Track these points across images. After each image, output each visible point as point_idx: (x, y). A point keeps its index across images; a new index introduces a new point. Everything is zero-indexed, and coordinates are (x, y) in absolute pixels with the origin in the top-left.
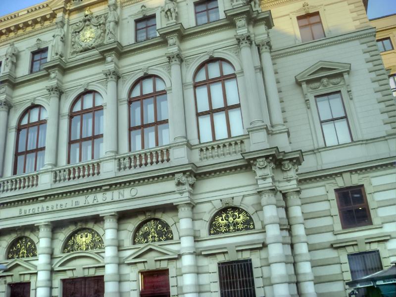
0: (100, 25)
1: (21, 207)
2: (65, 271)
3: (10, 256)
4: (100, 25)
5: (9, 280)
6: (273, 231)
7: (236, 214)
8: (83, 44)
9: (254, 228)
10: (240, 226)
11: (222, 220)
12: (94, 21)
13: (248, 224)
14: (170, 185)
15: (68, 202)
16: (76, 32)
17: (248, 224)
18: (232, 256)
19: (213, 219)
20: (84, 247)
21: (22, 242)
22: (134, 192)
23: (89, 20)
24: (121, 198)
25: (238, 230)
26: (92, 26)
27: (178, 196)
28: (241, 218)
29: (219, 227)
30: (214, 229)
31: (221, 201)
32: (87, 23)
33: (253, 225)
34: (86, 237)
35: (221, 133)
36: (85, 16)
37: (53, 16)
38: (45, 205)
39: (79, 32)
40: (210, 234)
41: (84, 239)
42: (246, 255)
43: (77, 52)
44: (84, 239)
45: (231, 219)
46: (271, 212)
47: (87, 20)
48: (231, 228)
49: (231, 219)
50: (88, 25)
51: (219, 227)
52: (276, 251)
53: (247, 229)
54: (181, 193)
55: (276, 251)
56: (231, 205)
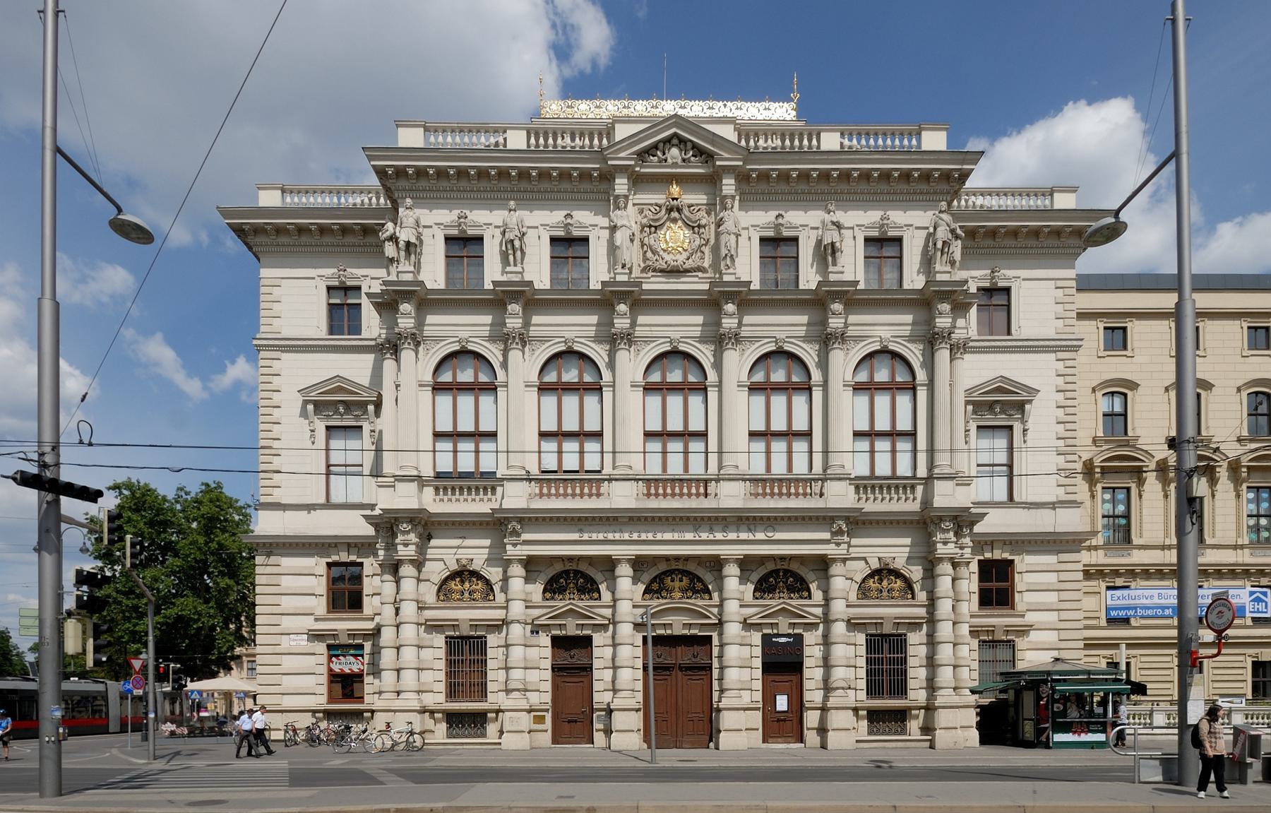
0: (699, 226)
4: (699, 226)
8: (668, 257)
10: (896, 594)
16: (650, 226)
19: (864, 580)
21: (568, 577)
23: (679, 210)
26: (680, 224)
27: (833, 546)
32: (675, 214)
34: (681, 580)
37: (607, 177)
47: (673, 209)
48: (885, 594)
50: (674, 221)
54: (838, 544)
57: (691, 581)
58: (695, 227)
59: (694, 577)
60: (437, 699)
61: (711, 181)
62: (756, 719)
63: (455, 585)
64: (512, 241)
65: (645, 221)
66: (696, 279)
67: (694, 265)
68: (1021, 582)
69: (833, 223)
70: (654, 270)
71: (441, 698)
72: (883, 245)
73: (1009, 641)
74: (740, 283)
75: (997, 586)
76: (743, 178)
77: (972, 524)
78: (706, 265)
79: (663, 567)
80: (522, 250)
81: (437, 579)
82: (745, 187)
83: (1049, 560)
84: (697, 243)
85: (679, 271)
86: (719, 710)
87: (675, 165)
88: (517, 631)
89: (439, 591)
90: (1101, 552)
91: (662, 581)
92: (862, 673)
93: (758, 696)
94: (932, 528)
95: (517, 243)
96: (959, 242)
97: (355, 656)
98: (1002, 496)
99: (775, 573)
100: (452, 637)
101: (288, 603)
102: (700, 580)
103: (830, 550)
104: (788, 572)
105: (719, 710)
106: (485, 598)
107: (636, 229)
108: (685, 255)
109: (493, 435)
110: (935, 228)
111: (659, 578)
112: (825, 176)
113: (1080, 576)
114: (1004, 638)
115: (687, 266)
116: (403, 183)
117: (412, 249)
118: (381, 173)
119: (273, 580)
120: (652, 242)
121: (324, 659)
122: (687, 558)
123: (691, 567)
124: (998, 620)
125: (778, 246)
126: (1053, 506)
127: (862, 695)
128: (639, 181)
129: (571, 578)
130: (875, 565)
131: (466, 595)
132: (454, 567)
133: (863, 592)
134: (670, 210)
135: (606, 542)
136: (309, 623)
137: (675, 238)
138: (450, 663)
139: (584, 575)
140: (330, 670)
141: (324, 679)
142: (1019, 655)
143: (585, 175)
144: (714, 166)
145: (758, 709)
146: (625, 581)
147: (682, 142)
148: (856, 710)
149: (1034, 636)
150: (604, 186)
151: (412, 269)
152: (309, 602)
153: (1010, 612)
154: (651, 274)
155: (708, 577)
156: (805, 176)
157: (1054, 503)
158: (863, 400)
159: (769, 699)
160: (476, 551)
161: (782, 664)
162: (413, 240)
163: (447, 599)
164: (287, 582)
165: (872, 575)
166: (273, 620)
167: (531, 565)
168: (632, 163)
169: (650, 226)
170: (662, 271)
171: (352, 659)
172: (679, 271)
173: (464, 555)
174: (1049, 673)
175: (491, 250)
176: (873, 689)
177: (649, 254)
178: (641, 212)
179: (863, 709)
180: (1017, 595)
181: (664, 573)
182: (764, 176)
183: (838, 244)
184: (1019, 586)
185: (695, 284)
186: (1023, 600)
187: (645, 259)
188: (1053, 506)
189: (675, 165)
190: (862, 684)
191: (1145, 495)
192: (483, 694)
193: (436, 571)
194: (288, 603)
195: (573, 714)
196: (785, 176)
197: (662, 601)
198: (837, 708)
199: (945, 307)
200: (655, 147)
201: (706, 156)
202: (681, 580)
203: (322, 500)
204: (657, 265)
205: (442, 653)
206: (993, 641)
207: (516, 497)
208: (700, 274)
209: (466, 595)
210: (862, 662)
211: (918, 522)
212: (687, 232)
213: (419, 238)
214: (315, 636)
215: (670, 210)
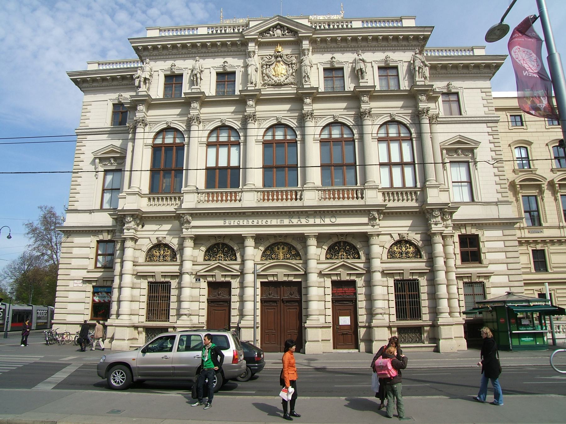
0: (292, 64)
2: (266, 275)
4: (292, 64)
7: (408, 245)
8: (275, 79)
11: (397, 248)
16: (267, 65)
18: (407, 277)
21: (219, 247)
23: (281, 57)
26: (281, 62)
31: (399, 234)
32: (279, 59)
35: (397, 183)
37: (245, 43)
39: (270, 65)
40: (388, 258)
45: (404, 249)
48: (404, 255)
49: (404, 249)
50: (279, 62)
56: (406, 238)
61: (298, 43)
62: (329, 334)
64: (196, 75)
66: (290, 88)
67: (289, 82)
68: (485, 246)
69: (360, 60)
70: (269, 85)
71: (143, 319)
72: (387, 69)
73: (481, 282)
74: (312, 88)
75: (471, 250)
76: (313, 41)
77: (451, 214)
79: (272, 241)
80: (201, 79)
81: (145, 249)
83: (498, 233)
84: (291, 71)
85: (281, 85)
86: (306, 328)
90: (526, 231)
92: (393, 304)
93: (330, 319)
94: (428, 215)
95: (198, 75)
96: (427, 68)
97: (107, 293)
98: (467, 199)
101: (75, 263)
102: (294, 248)
105: (306, 328)
106: (171, 260)
107: (259, 66)
108: (284, 77)
112: (355, 39)
113: (516, 243)
114: (477, 280)
115: (285, 82)
116: (146, 53)
118: (136, 49)
119: (69, 250)
120: (268, 72)
121: (90, 295)
122: (286, 236)
123: (289, 241)
124: (473, 270)
125: (333, 71)
126: (496, 204)
127: (393, 318)
128: (261, 45)
130: (397, 238)
131: (162, 258)
132: (155, 242)
133: (391, 254)
134: (276, 57)
136: (84, 274)
138: (150, 298)
139: (227, 246)
140: (93, 300)
141: (90, 306)
142: (487, 291)
143: (234, 44)
144: (298, 36)
147: (282, 27)
148: (390, 327)
149: (493, 279)
151: (146, 90)
152: (85, 262)
153: (480, 265)
155: (299, 247)
156: (344, 39)
157: (496, 202)
158: (383, 146)
161: (344, 296)
162: (148, 77)
163: (151, 261)
164: (76, 251)
166: (67, 272)
168: (257, 37)
169: (267, 65)
170: (272, 85)
171: (105, 295)
174: (505, 302)
176: (401, 314)
177: (266, 78)
178: (262, 59)
179: (394, 326)
180: (482, 254)
181: (273, 244)
182: (324, 40)
183: (364, 69)
184: (483, 250)
186: (487, 257)
187: (264, 80)
188: (496, 204)
189: (279, 37)
190: (393, 311)
191: (545, 200)
192: (167, 319)
194: (75, 263)
196: (334, 40)
197: (272, 261)
198: (377, 327)
199: (424, 98)
200: (269, 29)
201: (294, 33)
202: (283, 249)
203: (98, 207)
204: (270, 83)
205: (145, 292)
206: (471, 283)
208: (293, 86)
209: (162, 258)
210: (392, 297)
211: (420, 212)
213: (151, 76)
214: (86, 281)
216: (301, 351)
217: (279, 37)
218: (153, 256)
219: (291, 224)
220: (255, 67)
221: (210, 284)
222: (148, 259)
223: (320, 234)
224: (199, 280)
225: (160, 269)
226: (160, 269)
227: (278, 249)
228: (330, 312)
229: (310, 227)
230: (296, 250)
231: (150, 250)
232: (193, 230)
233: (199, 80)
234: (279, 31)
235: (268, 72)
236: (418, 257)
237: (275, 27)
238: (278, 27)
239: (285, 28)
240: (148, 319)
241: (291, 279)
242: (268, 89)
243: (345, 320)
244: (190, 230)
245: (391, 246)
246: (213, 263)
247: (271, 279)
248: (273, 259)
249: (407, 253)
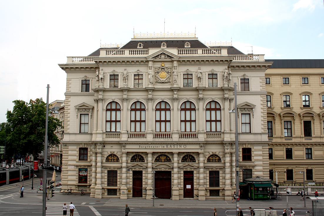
1: (140, 145)
3: (132, 161)
4: (169, 72)
5: (134, 170)
6: (228, 164)
8: (161, 79)
9: (221, 162)
12: (166, 69)
13: (219, 160)
14: (197, 147)
15: (160, 147)
16: (157, 72)
17: (219, 160)
19: (209, 157)
20: (163, 161)
21: (137, 156)
22: (185, 146)
23: (164, 69)
24: (180, 148)
25: (216, 162)
26: (165, 72)
27: (200, 150)
28: (217, 158)
29: (210, 160)
30: (209, 160)
32: (163, 70)
33: (221, 161)
34: (164, 157)
35: (213, 129)
36: (162, 67)
37: (148, 61)
38: (150, 146)
40: (207, 162)
41: (163, 158)
42: (218, 170)
43: (158, 82)
44: (163, 158)
45: (214, 158)
46: (228, 159)
49: (214, 158)
51: (210, 160)
52: (228, 170)
53: (219, 162)
55: (228, 170)
57: (167, 157)
58: (168, 73)
59: (167, 157)
60: (105, 186)
61: (172, 61)
62: (182, 192)
63: (110, 158)
65: (156, 71)
66: (168, 84)
70: (158, 82)
71: (106, 185)
72: (213, 76)
76: (179, 61)
78: (170, 81)
79: (159, 154)
80: (127, 79)
82: (179, 63)
84: (168, 76)
85: (164, 83)
87: (163, 59)
88: (124, 170)
89: (106, 159)
91: (159, 157)
92: (208, 181)
93: (182, 186)
95: (126, 78)
99: (187, 155)
100: (109, 171)
102: (169, 157)
103: (199, 151)
104: (190, 155)
106: (117, 161)
109: (120, 121)
110: (224, 73)
111: (159, 157)
115: (166, 82)
116: (100, 64)
117: (102, 79)
123: (166, 154)
125: (188, 76)
127: (208, 186)
129: (138, 157)
131: (113, 160)
132: (110, 153)
135: (146, 149)
137: (163, 75)
145: (182, 189)
146: (150, 158)
150: (146, 63)
154: (157, 83)
155: (170, 157)
159: (185, 186)
160: (115, 150)
161: (189, 177)
163: (108, 161)
165: (211, 156)
167: (128, 153)
172: (164, 83)
173: (112, 150)
175: (120, 78)
176: (211, 185)
177: (157, 79)
181: (160, 155)
183: (201, 77)
185: (167, 86)
187: (156, 80)
190: (208, 183)
192: (116, 185)
193: (106, 155)
195: (137, 190)
202: (164, 157)
207: (124, 138)
208: (169, 83)
209: (113, 160)
212: (166, 73)
215: (162, 69)
216: (171, 198)
217: (162, 59)
218: (109, 159)
219: (168, 148)
220: (152, 75)
221: (133, 172)
222: (107, 161)
223: (179, 152)
224: (129, 170)
225: (113, 165)
226: (113, 165)
227: (162, 157)
228: (182, 183)
229: (175, 149)
230: (170, 158)
231: (108, 157)
232: (126, 150)
233: (126, 80)
234: (163, 56)
235: (158, 76)
236: (220, 161)
237: (161, 54)
238: (163, 54)
239: (166, 55)
240: (108, 185)
241: (167, 170)
242: (158, 85)
243: (189, 187)
244: (125, 150)
245: (209, 157)
246: (135, 163)
247: (159, 170)
248: (160, 161)
249: (215, 160)
